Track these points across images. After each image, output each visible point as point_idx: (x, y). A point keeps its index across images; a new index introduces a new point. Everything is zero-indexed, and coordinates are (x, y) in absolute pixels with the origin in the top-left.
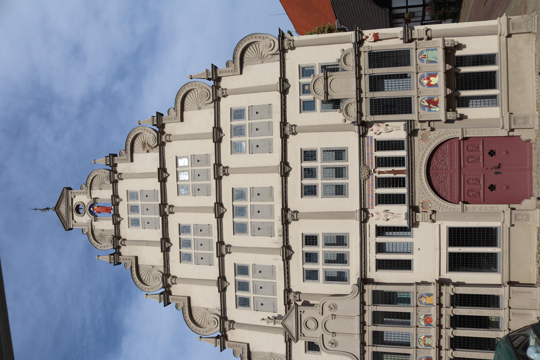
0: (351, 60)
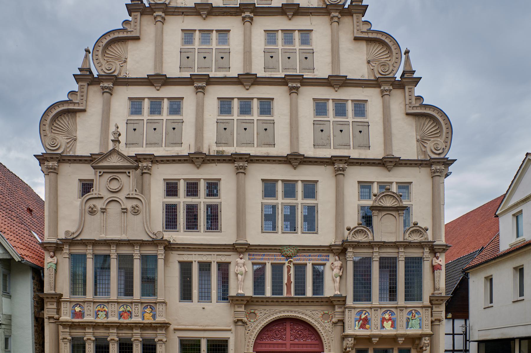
0: (416, 239)
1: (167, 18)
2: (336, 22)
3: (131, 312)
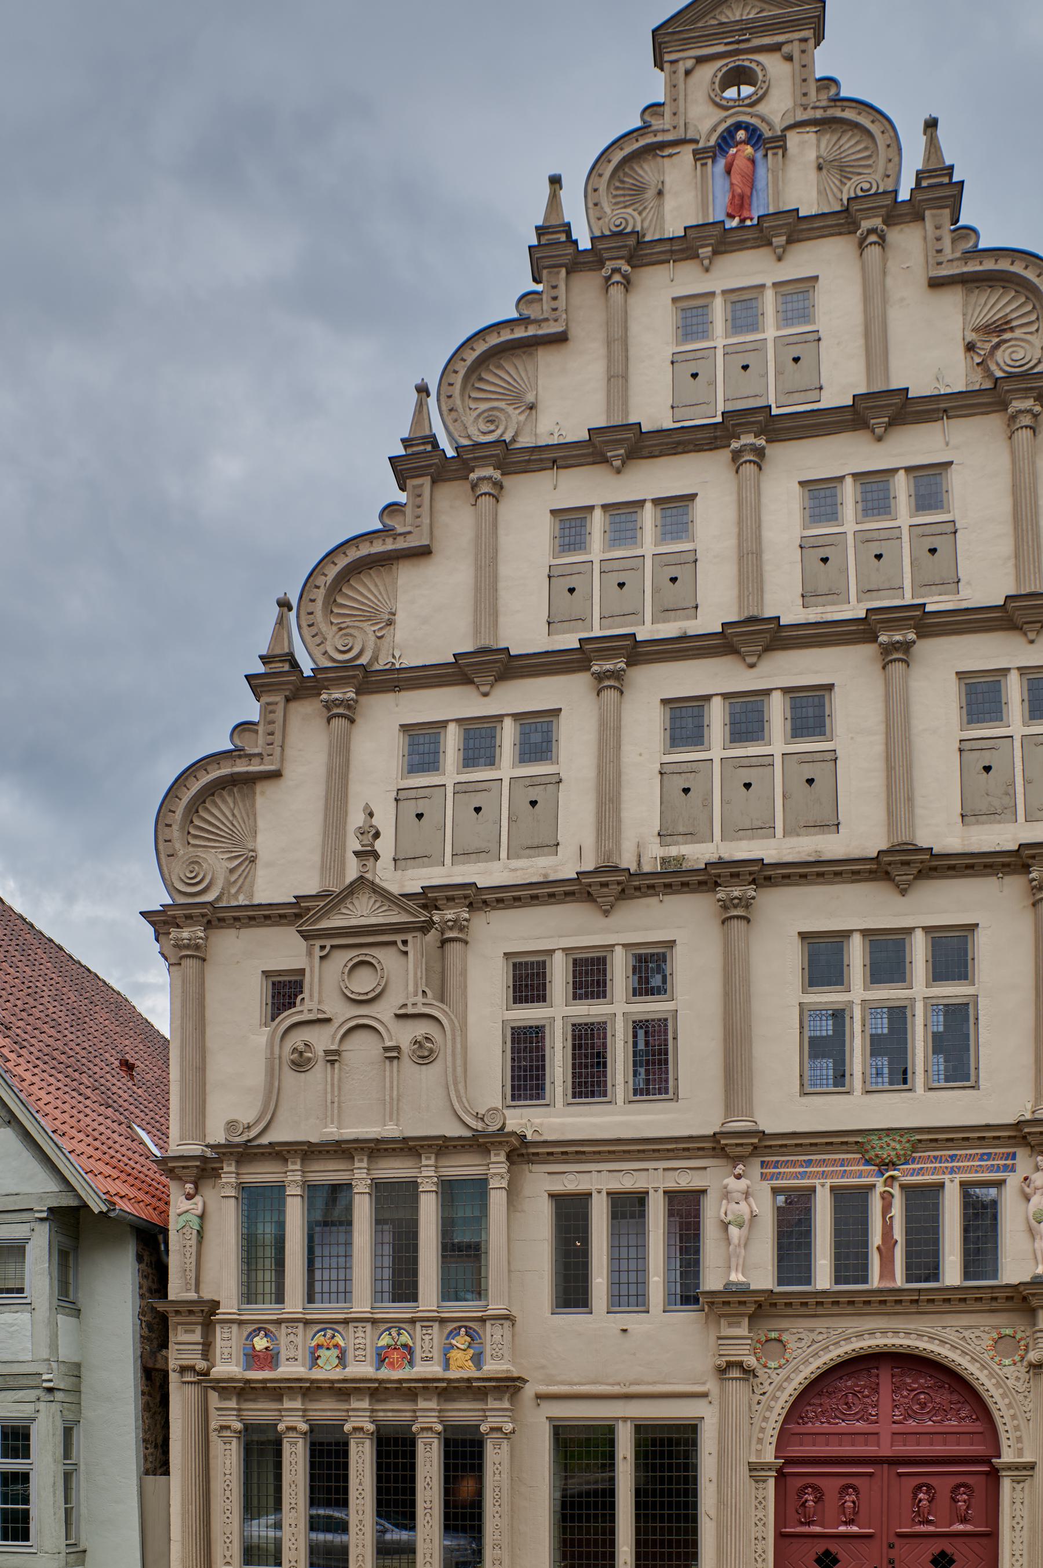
1: (508, 482)
2: (1026, 427)
3: (411, 1347)
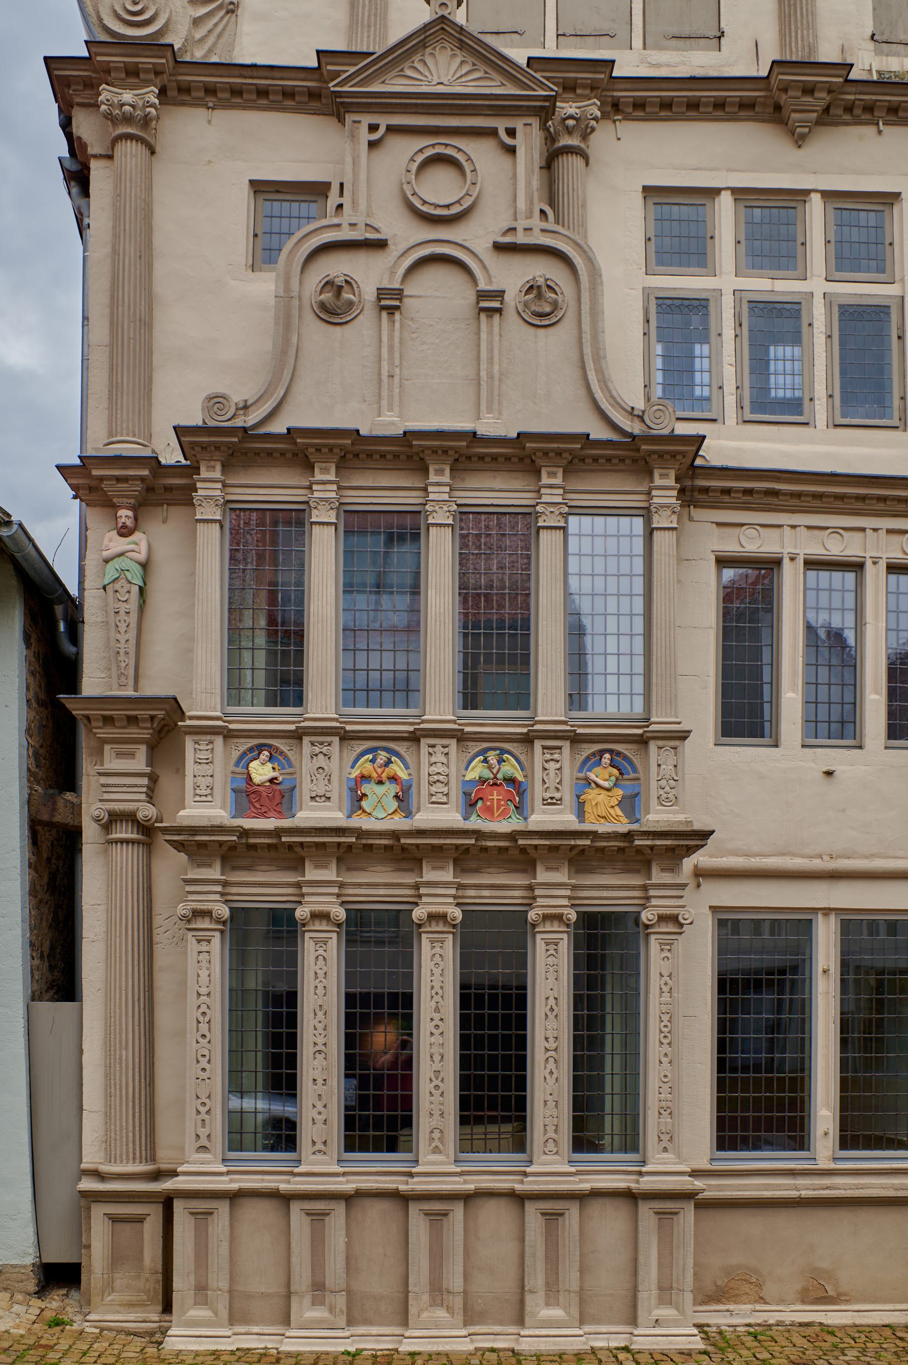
3: (520, 783)
